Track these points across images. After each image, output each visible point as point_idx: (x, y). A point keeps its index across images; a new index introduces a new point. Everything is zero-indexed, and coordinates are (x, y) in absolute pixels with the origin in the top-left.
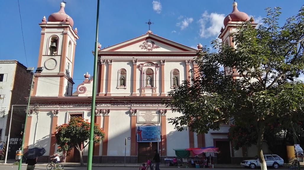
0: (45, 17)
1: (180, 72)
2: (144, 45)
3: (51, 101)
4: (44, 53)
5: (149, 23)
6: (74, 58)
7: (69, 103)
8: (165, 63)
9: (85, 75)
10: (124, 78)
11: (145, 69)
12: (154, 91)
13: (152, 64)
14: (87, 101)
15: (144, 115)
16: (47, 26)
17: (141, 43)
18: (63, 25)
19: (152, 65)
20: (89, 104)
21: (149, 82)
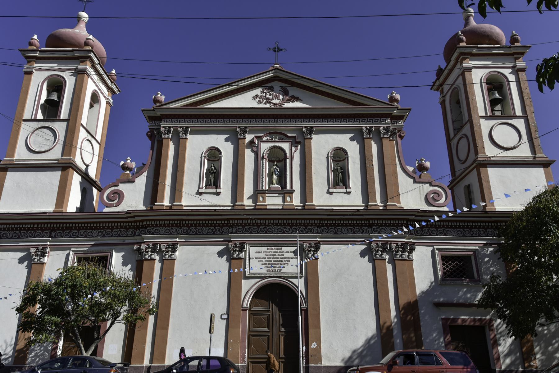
0: (35, 37)
1: (349, 154)
2: (264, 95)
3: (31, 224)
4: (27, 115)
5: (277, 50)
6: (105, 132)
7: (75, 227)
8: (314, 136)
9: (122, 163)
10: (215, 169)
11: (265, 147)
12: (288, 199)
13: (284, 137)
14: (123, 222)
15: (262, 255)
16: (37, 54)
17: (258, 91)
18: (77, 54)
19: (283, 139)
20: (127, 229)
21: (275, 177)
